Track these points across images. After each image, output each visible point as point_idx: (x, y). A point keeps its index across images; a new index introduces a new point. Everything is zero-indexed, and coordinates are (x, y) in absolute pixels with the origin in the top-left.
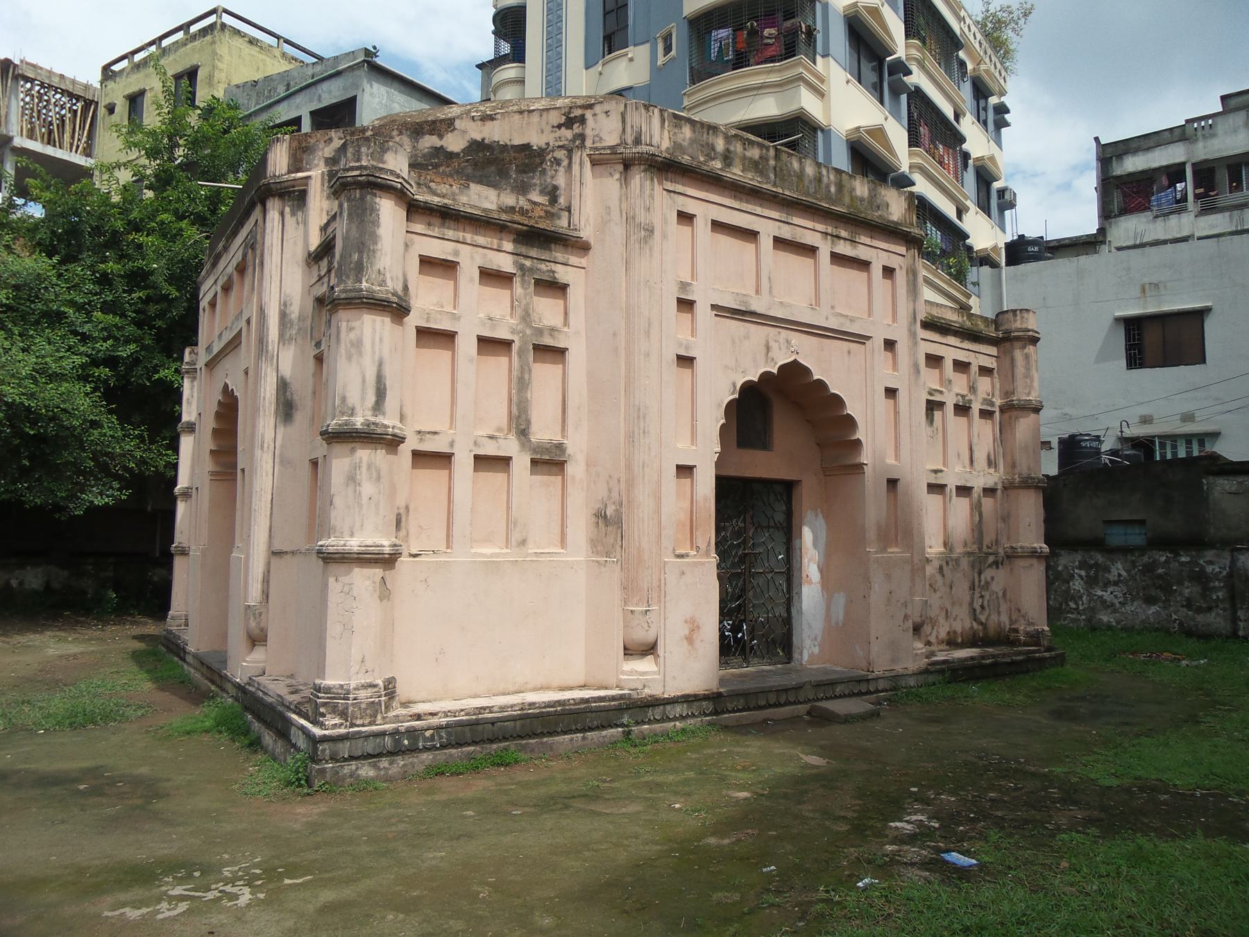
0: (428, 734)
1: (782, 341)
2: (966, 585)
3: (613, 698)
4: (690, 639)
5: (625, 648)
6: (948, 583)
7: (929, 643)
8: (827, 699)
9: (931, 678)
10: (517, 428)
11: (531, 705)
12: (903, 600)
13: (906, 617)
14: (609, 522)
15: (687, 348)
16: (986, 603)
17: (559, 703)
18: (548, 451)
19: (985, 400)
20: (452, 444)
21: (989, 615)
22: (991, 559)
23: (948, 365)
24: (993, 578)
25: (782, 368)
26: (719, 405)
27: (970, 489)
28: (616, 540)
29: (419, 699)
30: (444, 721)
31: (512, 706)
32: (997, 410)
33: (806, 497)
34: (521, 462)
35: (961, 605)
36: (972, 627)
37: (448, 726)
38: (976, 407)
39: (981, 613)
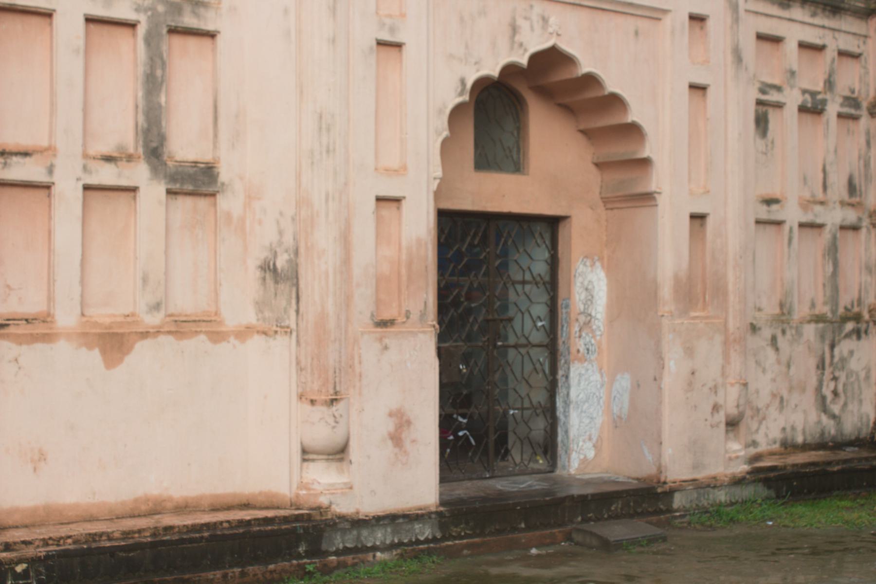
0: (19, 569)
1: (535, 18)
2: (812, 362)
3: (286, 520)
4: (396, 439)
5: (304, 451)
6: (784, 359)
7: (754, 444)
8: (597, 520)
9: (747, 492)
10: (146, 145)
11: (168, 529)
12: (711, 384)
13: (716, 408)
14: (280, 275)
15: (392, 30)
16: (840, 388)
17: (207, 525)
18: (192, 178)
19: (846, 98)
20: (50, 170)
21: (845, 404)
22: (850, 326)
23: (791, 46)
24: (851, 353)
25: (535, 58)
26: (440, 112)
27: (820, 226)
28: (289, 303)
29: (11, 522)
30: (42, 552)
31: (139, 531)
32: (864, 112)
33: (577, 241)
34: (153, 192)
35: (803, 390)
37: (48, 557)
38: (833, 108)
39: (833, 401)
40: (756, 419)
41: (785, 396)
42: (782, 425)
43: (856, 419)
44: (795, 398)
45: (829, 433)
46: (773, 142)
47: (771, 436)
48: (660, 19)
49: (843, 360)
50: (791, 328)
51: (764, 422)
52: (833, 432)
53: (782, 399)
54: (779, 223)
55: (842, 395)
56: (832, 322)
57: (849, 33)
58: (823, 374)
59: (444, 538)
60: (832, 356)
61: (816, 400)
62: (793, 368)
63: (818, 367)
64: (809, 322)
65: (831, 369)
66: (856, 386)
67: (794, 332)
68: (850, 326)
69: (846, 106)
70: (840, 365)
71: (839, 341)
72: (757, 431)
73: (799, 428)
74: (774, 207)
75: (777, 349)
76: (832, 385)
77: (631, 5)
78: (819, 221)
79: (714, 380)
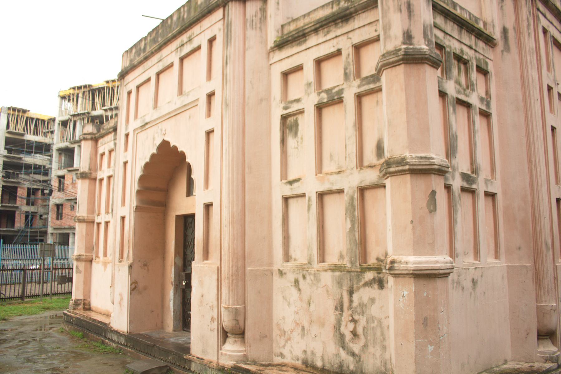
2: (331, 304)
6: (305, 298)
12: (210, 304)
16: (360, 330)
21: (366, 346)
22: (369, 276)
24: (373, 300)
27: (340, 191)
35: (323, 325)
36: (337, 355)
39: (352, 340)
40: (283, 337)
41: (306, 327)
42: (304, 348)
43: (378, 363)
44: (315, 330)
45: (348, 367)
46: (302, 138)
47: (294, 354)
48: (197, 105)
49: (362, 305)
50: (310, 274)
51: (289, 342)
52: (352, 367)
53: (303, 328)
54: (303, 195)
55: (362, 337)
56: (349, 271)
57: (364, 26)
58: (342, 315)
59: (127, 346)
60: (351, 301)
61: (334, 335)
62: (312, 306)
63: (336, 308)
64: (326, 271)
65: (350, 312)
66: (378, 333)
67: (312, 277)
68: (369, 276)
69: (364, 85)
70: (359, 310)
71: (358, 289)
72: (284, 346)
73: (319, 354)
74: (296, 185)
75: (299, 290)
76: (351, 326)
77: (185, 105)
78: (335, 187)
79: (212, 302)
